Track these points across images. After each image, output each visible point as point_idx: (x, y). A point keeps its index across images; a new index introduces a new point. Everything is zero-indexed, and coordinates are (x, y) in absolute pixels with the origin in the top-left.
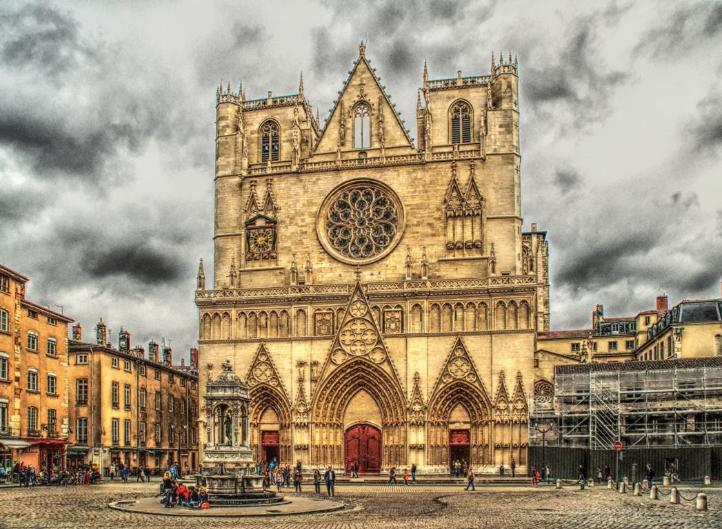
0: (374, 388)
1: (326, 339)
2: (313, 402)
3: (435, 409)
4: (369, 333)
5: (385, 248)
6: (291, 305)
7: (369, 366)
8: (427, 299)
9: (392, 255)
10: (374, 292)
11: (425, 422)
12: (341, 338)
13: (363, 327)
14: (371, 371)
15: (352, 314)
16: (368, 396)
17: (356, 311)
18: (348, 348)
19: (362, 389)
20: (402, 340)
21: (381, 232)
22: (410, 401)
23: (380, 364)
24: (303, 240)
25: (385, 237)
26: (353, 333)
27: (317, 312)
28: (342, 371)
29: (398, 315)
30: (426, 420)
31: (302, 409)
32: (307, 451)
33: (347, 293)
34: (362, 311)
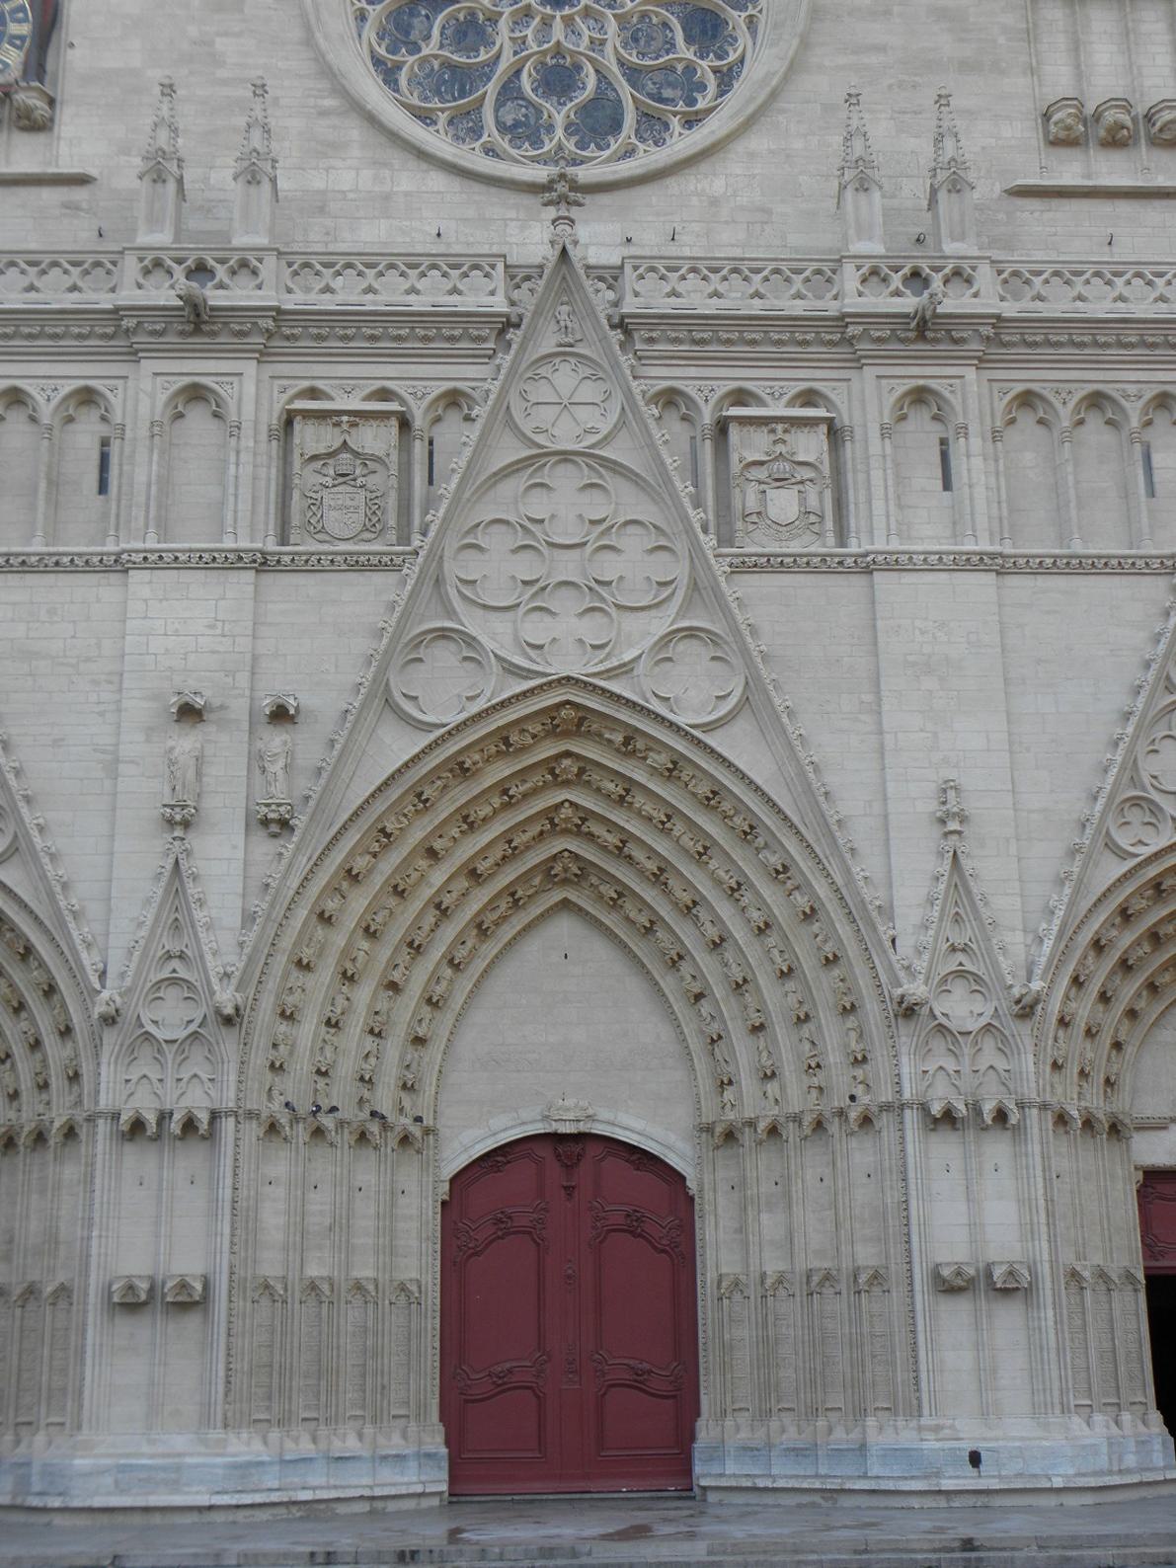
0: (649, 894)
1: (358, 565)
2: (252, 977)
3: (1063, 1023)
4: (634, 543)
5: (690, 122)
6: (133, 355)
7: (631, 744)
8: (982, 362)
9: (740, 147)
10: (665, 306)
11: (1021, 1106)
12: (453, 569)
13: (597, 507)
14: (640, 776)
15: (527, 427)
16: (600, 951)
17: (550, 412)
18: (501, 625)
19: (565, 904)
20: (848, 589)
21: (671, 46)
22: (921, 964)
23: (709, 727)
24: (220, 44)
25: (690, 69)
26: (530, 538)
27: (299, 405)
28: (461, 770)
29: (810, 446)
30: (1030, 1092)
31: (171, 1018)
32: (192, 1322)
33: (499, 304)
34: (581, 412)
